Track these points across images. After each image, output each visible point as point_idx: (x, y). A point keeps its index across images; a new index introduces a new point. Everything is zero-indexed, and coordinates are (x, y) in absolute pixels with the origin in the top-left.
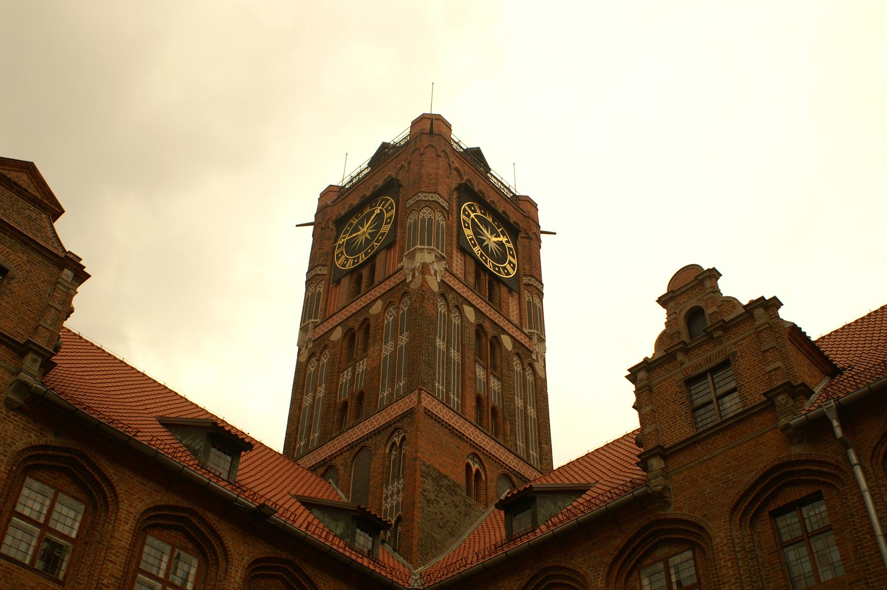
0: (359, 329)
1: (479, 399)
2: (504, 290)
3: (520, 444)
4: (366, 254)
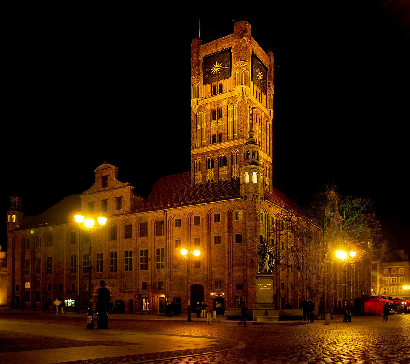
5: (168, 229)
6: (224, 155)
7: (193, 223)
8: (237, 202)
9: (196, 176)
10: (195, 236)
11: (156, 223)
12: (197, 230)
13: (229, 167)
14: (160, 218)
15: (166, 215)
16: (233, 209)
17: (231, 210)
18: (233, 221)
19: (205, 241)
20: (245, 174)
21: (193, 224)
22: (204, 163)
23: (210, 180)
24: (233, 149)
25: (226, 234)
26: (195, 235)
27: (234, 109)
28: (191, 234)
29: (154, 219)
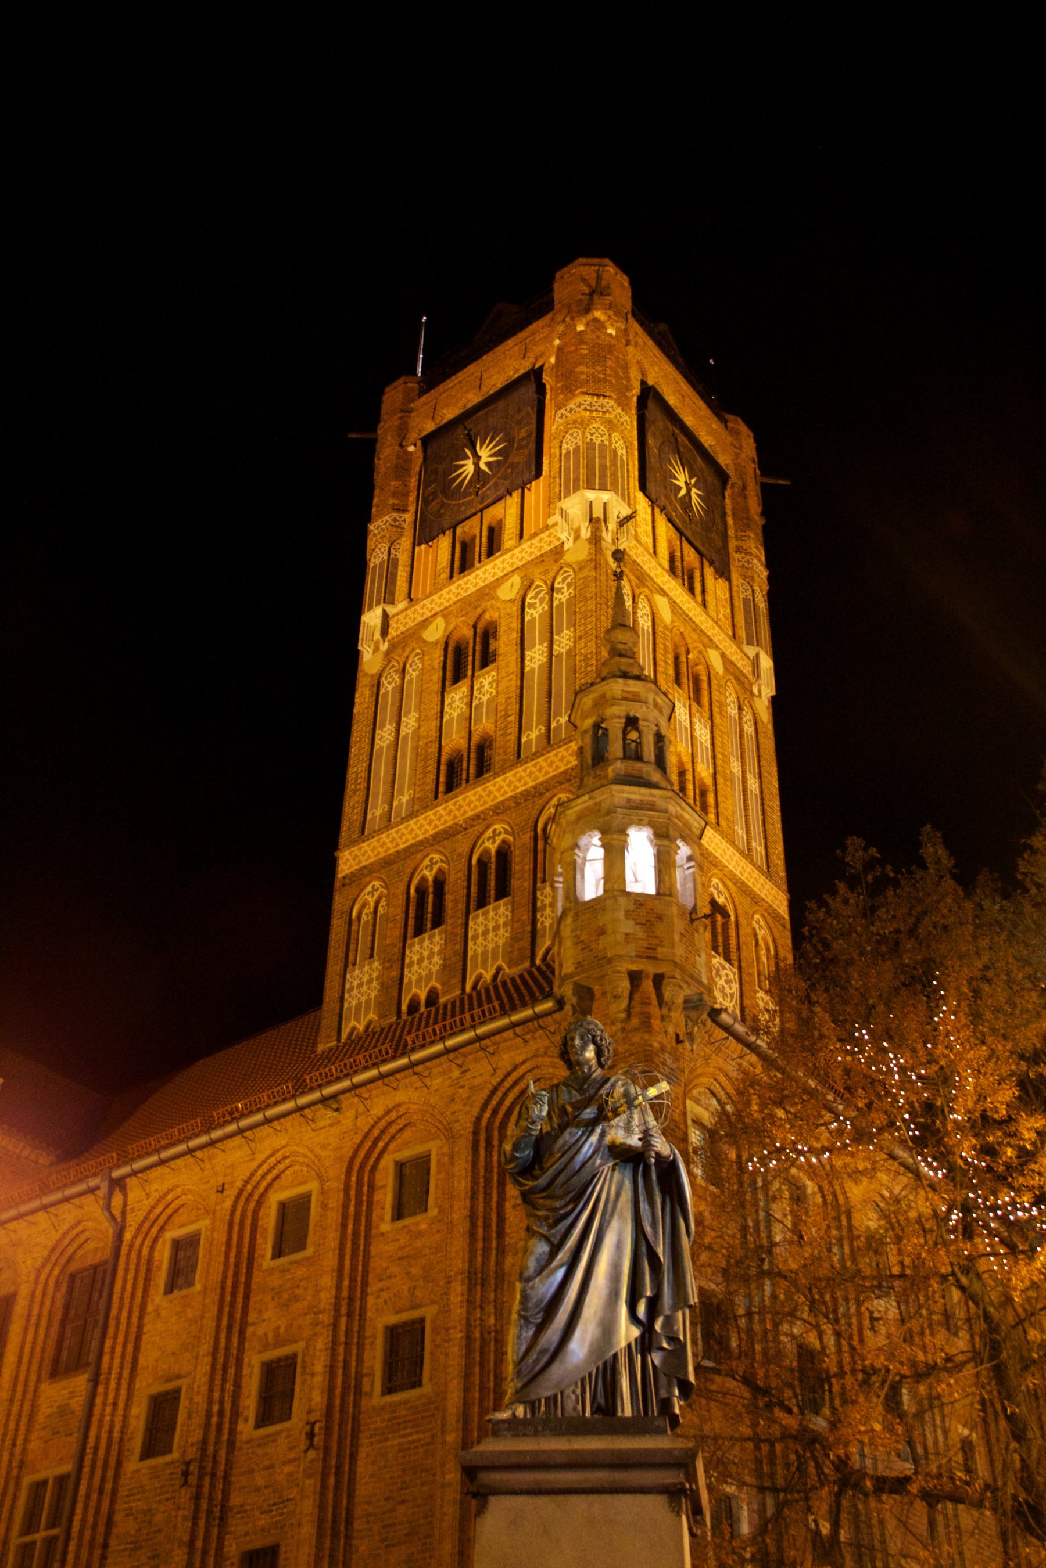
5: (114, 1312)
6: (498, 840)
7: (266, 1246)
8: (533, 1046)
9: (351, 989)
10: (265, 1348)
11: (64, 1288)
12: (285, 1295)
13: (523, 898)
14: (91, 1245)
15: (123, 1213)
17: (495, 1112)
20: (577, 846)
21: (263, 1256)
22: (398, 912)
23: (423, 996)
24: (544, 799)
25: (458, 1288)
26: (270, 1336)
27: (551, 607)
28: (242, 1333)
29: (54, 1258)
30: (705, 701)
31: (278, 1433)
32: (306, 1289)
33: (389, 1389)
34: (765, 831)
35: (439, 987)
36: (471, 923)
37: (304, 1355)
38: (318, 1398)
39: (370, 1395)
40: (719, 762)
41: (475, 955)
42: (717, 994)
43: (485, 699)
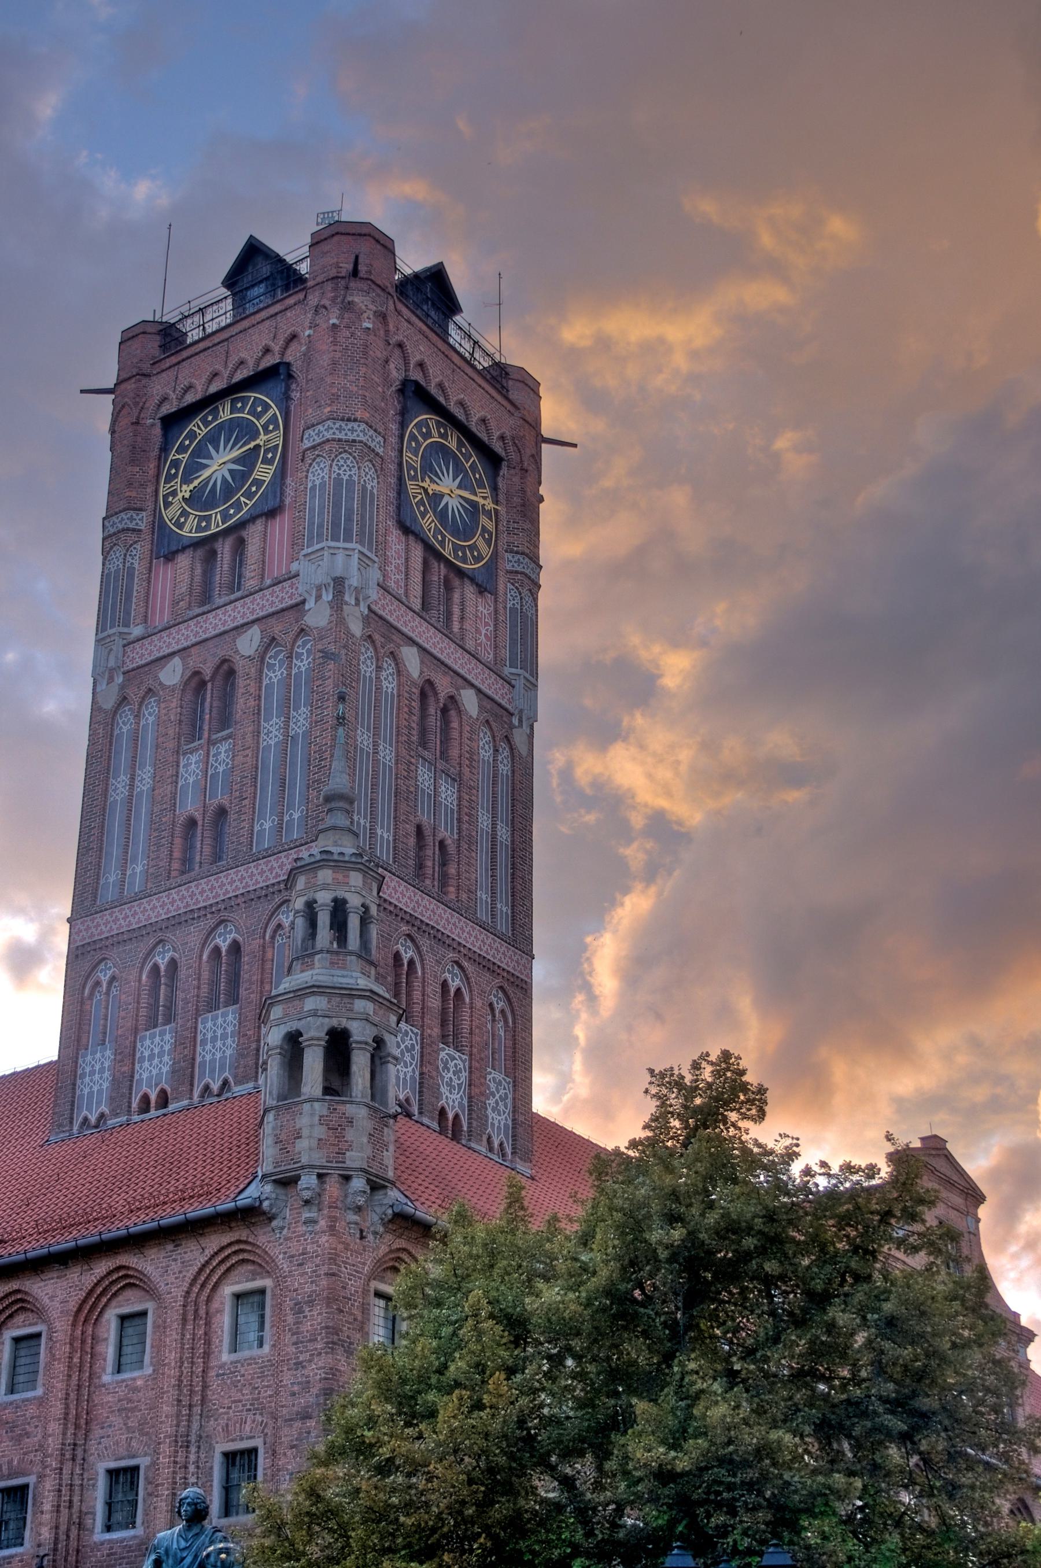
0: (213, 678)
1: (419, 829)
2: (470, 590)
3: (483, 895)
4: (225, 517)
16: (214, 1279)
18: (213, 1363)
19: (47, 1507)
23: (153, 1097)
27: (289, 675)
30: (454, 752)
31: (12, 1557)
32: (36, 1427)
33: (108, 1528)
34: (513, 888)
35: (169, 1090)
36: (200, 1027)
37: (35, 1488)
38: (46, 1534)
39: (92, 1531)
40: (465, 826)
41: (203, 1064)
42: (444, 1090)
43: (221, 769)
